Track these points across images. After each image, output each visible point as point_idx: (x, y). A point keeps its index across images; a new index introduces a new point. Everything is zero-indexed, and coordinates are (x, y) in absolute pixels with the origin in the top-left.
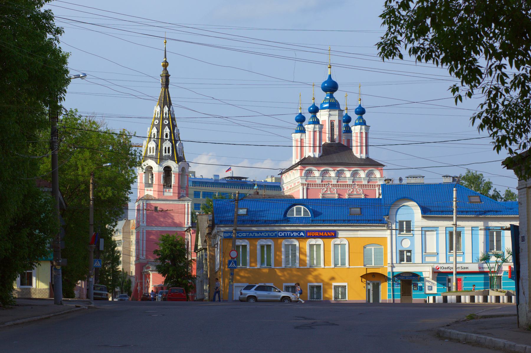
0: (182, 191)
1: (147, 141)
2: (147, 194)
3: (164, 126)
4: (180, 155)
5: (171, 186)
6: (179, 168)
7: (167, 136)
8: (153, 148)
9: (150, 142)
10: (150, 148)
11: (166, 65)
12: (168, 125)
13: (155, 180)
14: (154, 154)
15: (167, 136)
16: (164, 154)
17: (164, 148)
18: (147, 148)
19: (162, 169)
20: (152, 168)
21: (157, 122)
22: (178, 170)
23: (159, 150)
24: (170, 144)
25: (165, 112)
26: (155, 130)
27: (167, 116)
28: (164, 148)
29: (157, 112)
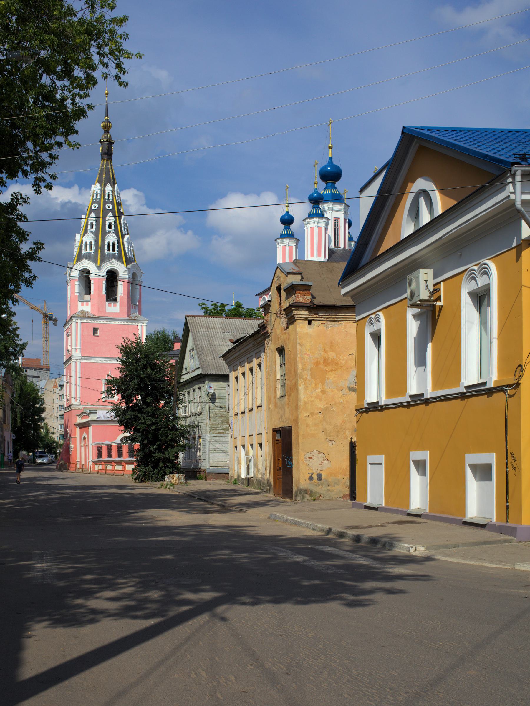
0: (132, 306)
1: (81, 235)
2: (82, 311)
3: (106, 212)
4: (129, 255)
5: (115, 300)
6: (129, 272)
8: (91, 243)
9: (86, 235)
10: (86, 243)
11: (107, 128)
12: (113, 210)
13: (94, 290)
14: (93, 251)
16: (106, 252)
17: (106, 243)
18: (82, 243)
19: (103, 272)
20: (89, 272)
21: (95, 207)
22: (127, 276)
23: (99, 246)
24: (116, 237)
25: (107, 192)
27: (111, 197)
28: (106, 243)
29: (95, 192)
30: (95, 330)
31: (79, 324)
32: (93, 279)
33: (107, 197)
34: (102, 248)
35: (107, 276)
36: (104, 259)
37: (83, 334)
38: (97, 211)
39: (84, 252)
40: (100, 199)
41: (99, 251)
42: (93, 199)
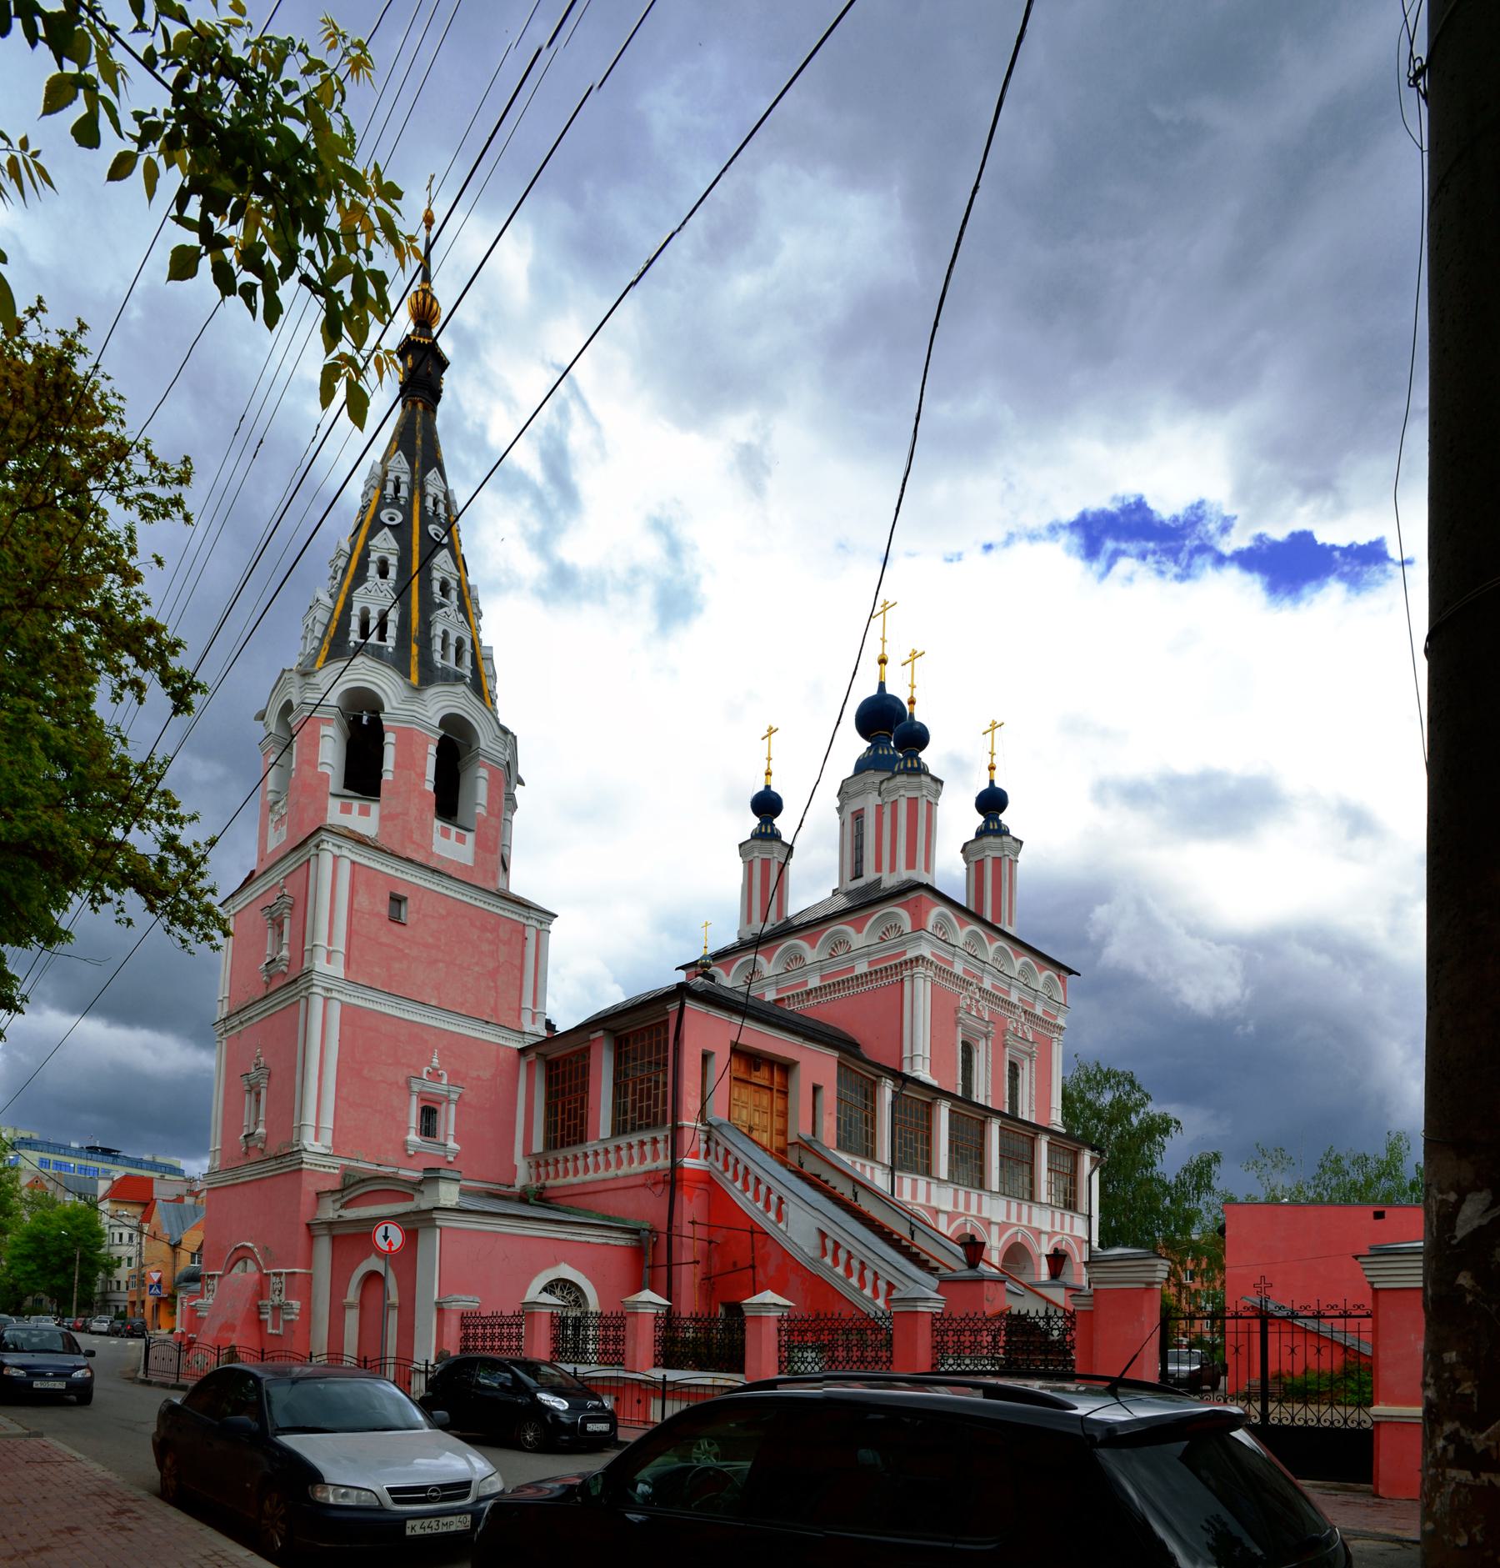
8: (383, 617)
10: (365, 613)
16: (437, 657)
17: (438, 630)
21: (392, 519)
26: (385, 544)
27: (441, 509)
30: (397, 900)
32: (395, 730)
33: (429, 502)
37: (355, 906)
38: (401, 532)
39: (354, 636)
40: (410, 502)
41: (415, 649)
42: (382, 497)
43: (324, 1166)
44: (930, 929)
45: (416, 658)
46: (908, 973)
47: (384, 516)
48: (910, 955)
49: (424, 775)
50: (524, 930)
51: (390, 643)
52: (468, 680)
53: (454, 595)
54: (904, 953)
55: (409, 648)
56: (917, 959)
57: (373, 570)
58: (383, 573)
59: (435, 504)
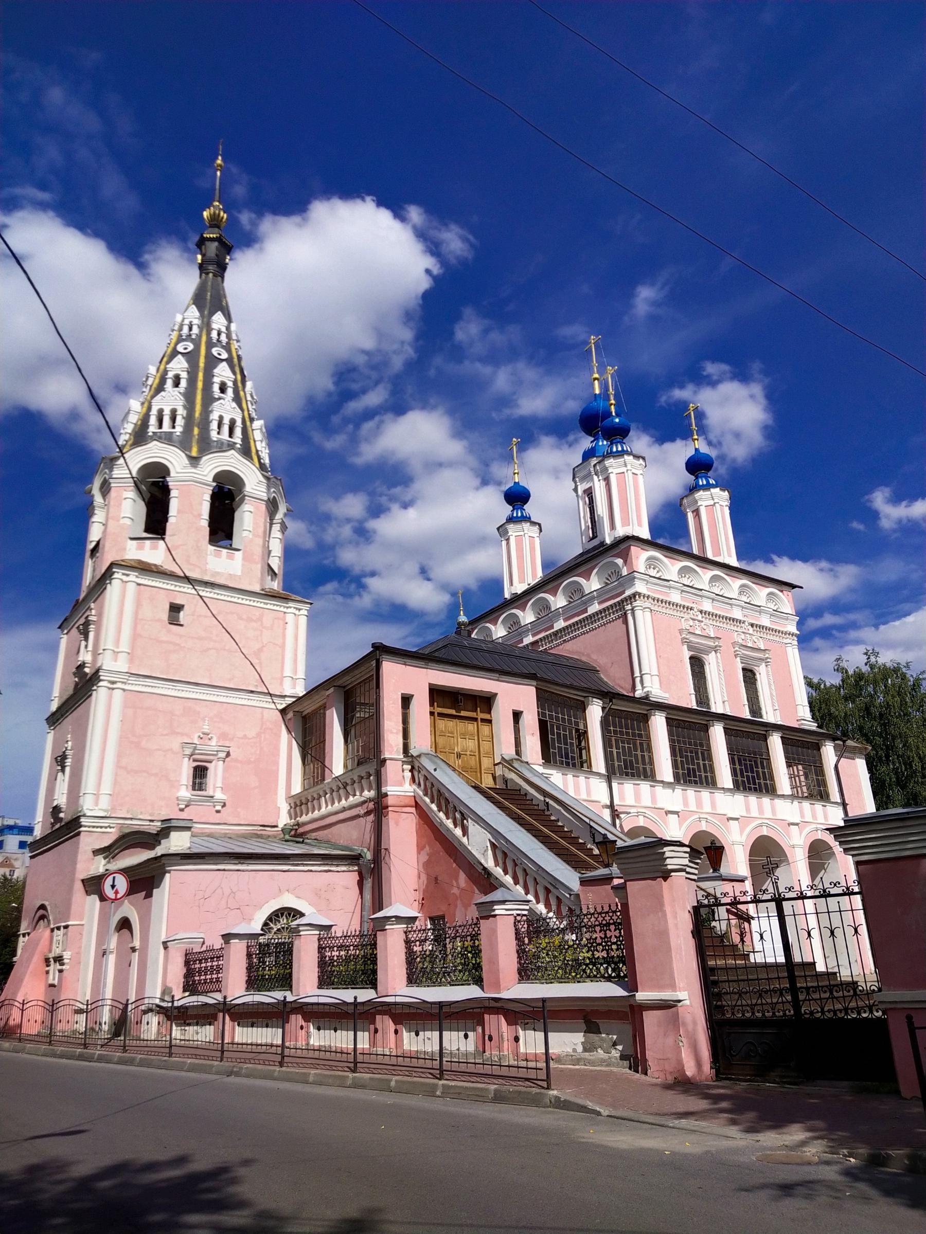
3: (213, 362)
7: (223, 389)
9: (163, 393)
10: (160, 413)
15: (223, 389)
16: (214, 435)
17: (214, 416)
21: (185, 349)
26: (179, 366)
27: (223, 338)
30: (175, 609)
31: (131, 587)
33: (214, 335)
34: (205, 424)
35: (215, 484)
36: (206, 446)
37: (140, 617)
38: (191, 357)
39: (152, 428)
40: (199, 336)
41: (196, 431)
42: (180, 336)
43: (101, 827)
44: (642, 570)
45: (197, 437)
46: (629, 607)
47: (180, 348)
48: (628, 593)
49: (200, 515)
50: (285, 617)
51: (179, 429)
52: (238, 446)
53: (230, 391)
54: (623, 592)
55: (192, 430)
56: (634, 595)
57: (169, 383)
58: (177, 384)
59: (219, 334)
